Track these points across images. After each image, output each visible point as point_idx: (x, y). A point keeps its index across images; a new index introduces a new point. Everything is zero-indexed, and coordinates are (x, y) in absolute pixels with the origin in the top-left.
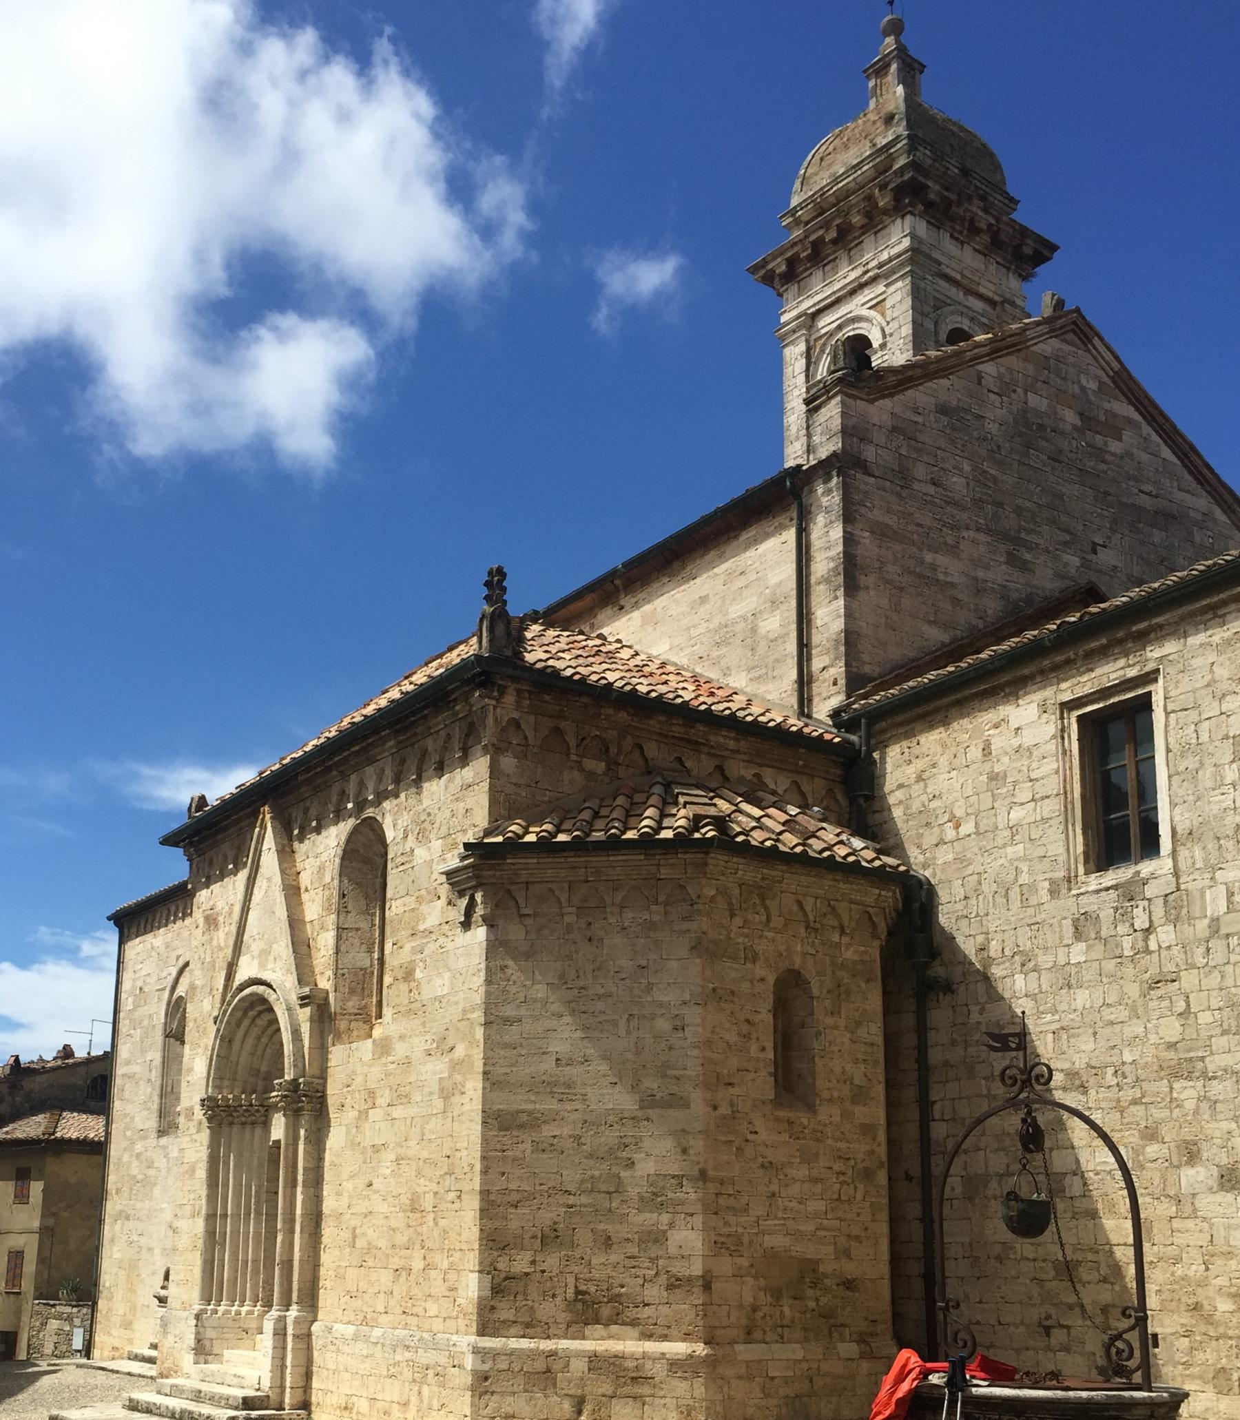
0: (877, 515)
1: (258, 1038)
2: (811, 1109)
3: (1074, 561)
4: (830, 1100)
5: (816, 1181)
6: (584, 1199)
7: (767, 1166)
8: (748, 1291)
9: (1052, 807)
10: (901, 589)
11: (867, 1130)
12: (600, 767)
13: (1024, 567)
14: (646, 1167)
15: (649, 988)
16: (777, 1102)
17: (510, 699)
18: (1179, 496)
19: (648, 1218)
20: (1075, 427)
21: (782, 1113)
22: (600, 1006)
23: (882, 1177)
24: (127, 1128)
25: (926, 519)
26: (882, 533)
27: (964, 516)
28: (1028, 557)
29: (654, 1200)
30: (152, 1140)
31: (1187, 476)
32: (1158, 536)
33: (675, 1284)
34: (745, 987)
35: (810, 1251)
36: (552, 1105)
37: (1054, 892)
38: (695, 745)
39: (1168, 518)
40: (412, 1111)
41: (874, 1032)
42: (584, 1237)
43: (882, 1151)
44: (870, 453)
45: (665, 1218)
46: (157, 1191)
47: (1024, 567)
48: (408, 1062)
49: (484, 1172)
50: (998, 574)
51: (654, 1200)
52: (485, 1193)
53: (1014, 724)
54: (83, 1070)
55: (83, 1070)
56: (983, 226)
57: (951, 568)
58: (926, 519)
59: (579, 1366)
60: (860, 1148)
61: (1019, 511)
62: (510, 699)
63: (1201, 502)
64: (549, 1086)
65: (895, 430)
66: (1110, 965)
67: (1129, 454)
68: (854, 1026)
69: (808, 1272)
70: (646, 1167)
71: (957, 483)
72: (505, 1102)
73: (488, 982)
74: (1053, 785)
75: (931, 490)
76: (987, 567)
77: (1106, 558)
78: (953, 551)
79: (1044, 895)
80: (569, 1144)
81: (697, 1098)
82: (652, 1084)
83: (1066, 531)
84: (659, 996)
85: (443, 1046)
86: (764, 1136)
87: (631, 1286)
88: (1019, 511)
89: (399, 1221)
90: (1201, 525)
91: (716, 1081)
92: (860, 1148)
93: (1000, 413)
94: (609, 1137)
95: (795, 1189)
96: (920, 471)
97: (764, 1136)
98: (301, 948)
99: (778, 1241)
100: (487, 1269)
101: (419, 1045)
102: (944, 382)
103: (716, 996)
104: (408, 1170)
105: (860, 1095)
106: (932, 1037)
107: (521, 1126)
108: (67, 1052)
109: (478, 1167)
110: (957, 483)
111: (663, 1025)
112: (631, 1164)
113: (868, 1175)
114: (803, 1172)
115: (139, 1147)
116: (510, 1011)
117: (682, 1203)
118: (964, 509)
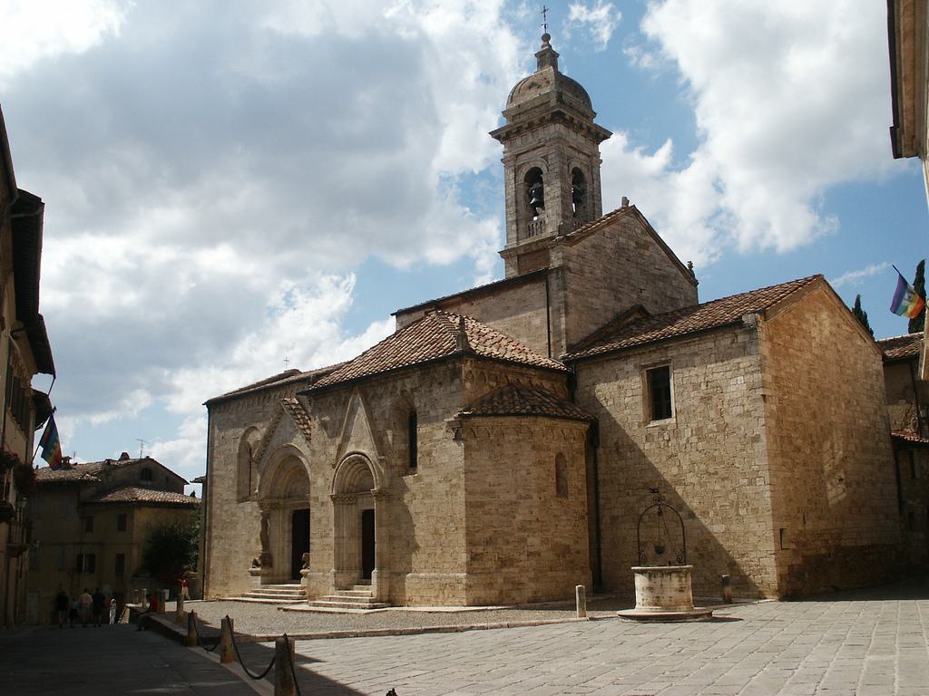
0: (574, 287)
1: (353, 474)
2: (567, 498)
3: (636, 296)
4: (572, 494)
5: (569, 520)
6: (500, 529)
7: (554, 516)
8: (551, 556)
9: (639, 399)
10: (582, 312)
11: (582, 503)
12: (494, 384)
13: (620, 300)
14: (519, 518)
15: (519, 460)
16: (557, 496)
17: (469, 364)
18: (668, 269)
19: (522, 534)
20: (635, 248)
21: (559, 499)
22: (503, 467)
23: (587, 517)
24: (218, 498)
25: (588, 286)
26: (576, 293)
27: (601, 284)
28: (620, 296)
29: (522, 529)
30: (234, 505)
31: (670, 262)
32: (661, 284)
33: (530, 554)
34: (547, 459)
35: (567, 542)
36: (486, 499)
37: (639, 426)
38: (522, 375)
39: (664, 278)
40: (433, 501)
41: (583, 471)
42: (500, 541)
43: (586, 509)
44: (571, 265)
45: (526, 534)
46: (239, 526)
47: (620, 300)
48: (431, 484)
49: (467, 521)
50: (611, 304)
51: (522, 529)
52: (467, 528)
53: (626, 370)
54: (137, 466)
55: (137, 466)
56: (585, 127)
57: (597, 303)
58: (588, 286)
59: (500, 580)
60: (580, 509)
61: (617, 280)
62: (469, 364)
63: (675, 270)
64: (485, 493)
65: (579, 256)
66: (657, 451)
67: (651, 256)
68: (578, 470)
69: (567, 547)
70: (519, 518)
71: (598, 272)
72: (472, 499)
73: (465, 459)
74: (640, 391)
75: (590, 275)
76: (608, 302)
77: (644, 294)
78: (597, 297)
79: (636, 428)
80: (493, 511)
81: (535, 496)
82: (520, 491)
83: (632, 285)
84: (522, 463)
85: (446, 479)
86: (554, 507)
87: (516, 556)
88: (617, 280)
89: (429, 537)
90: (675, 278)
91: (541, 490)
92: (580, 509)
93: (611, 246)
94: (508, 509)
95: (562, 523)
96: (587, 269)
97: (554, 507)
98: (379, 440)
99: (559, 540)
100: (469, 551)
101: (435, 479)
102: (593, 236)
103: (540, 463)
104: (433, 521)
105: (580, 492)
106: (599, 471)
107: (479, 507)
108: (125, 456)
109: (464, 519)
110: (598, 272)
111: (524, 472)
112: (515, 517)
113: (583, 517)
114: (564, 517)
115: (226, 507)
116: (473, 469)
117: (532, 529)
118: (600, 281)
